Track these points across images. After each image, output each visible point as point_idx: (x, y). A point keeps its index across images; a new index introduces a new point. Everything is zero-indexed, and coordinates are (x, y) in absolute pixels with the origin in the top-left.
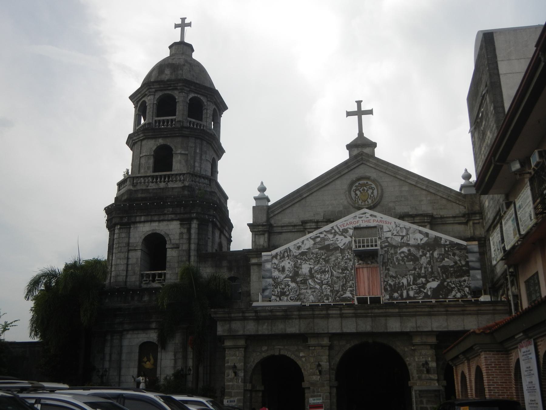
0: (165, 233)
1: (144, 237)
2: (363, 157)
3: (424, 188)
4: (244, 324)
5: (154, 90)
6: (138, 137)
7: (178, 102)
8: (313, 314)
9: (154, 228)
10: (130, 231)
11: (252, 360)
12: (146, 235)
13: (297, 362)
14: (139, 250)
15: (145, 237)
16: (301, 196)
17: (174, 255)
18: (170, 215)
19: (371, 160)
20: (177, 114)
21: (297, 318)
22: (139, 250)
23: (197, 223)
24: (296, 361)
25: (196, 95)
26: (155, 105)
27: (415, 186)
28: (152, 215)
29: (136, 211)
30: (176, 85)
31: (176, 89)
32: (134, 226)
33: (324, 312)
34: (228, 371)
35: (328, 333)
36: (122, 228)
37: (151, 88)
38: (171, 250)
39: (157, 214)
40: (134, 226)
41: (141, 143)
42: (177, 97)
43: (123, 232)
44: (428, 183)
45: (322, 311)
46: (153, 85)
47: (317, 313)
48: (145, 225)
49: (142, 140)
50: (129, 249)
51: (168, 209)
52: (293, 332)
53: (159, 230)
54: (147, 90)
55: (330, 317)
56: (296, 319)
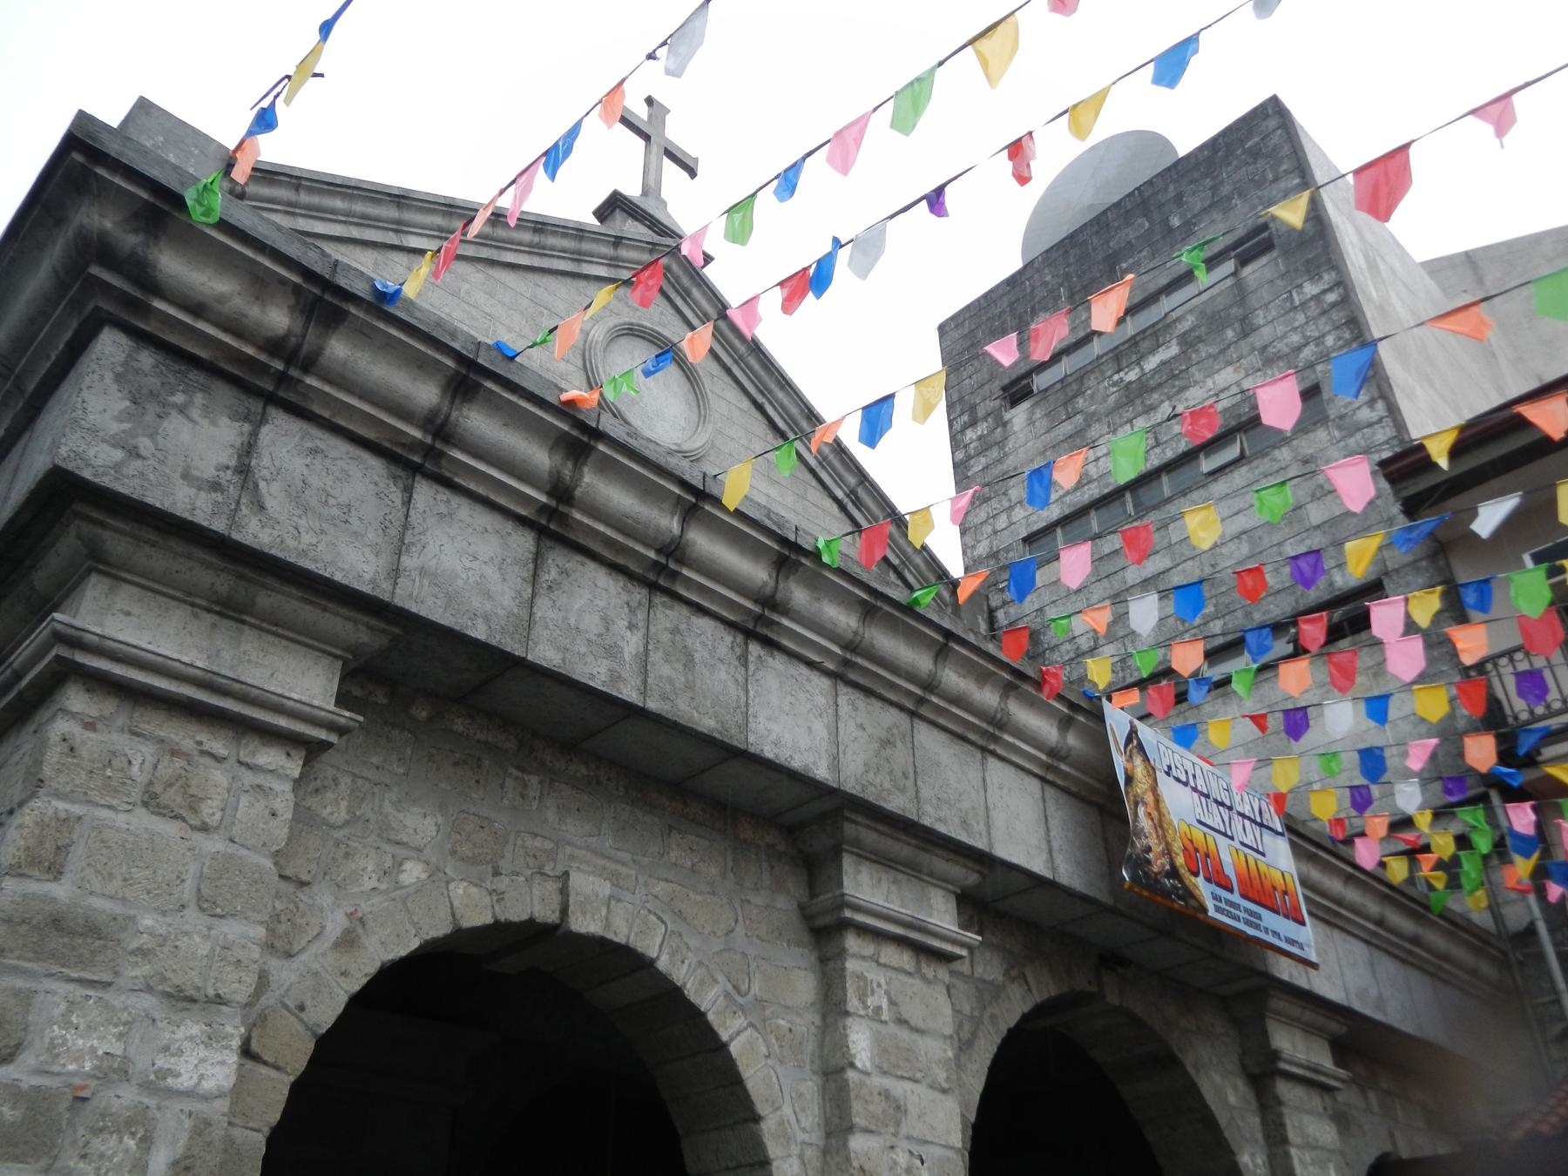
2: (675, 267)
3: (840, 494)
4: (408, 502)
8: (930, 685)
11: (335, 924)
13: (734, 1049)
16: (397, 231)
19: (696, 293)
21: (830, 666)
24: (725, 1037)
27: (812, 471)
33: (988, 697)
34: (20, 983)
35: (983, 860)
44: (861, 483)
45: (983, 678)
47: (952, 678)
52: (797, 764)
55: (1000, 751)
56: (811, 664)
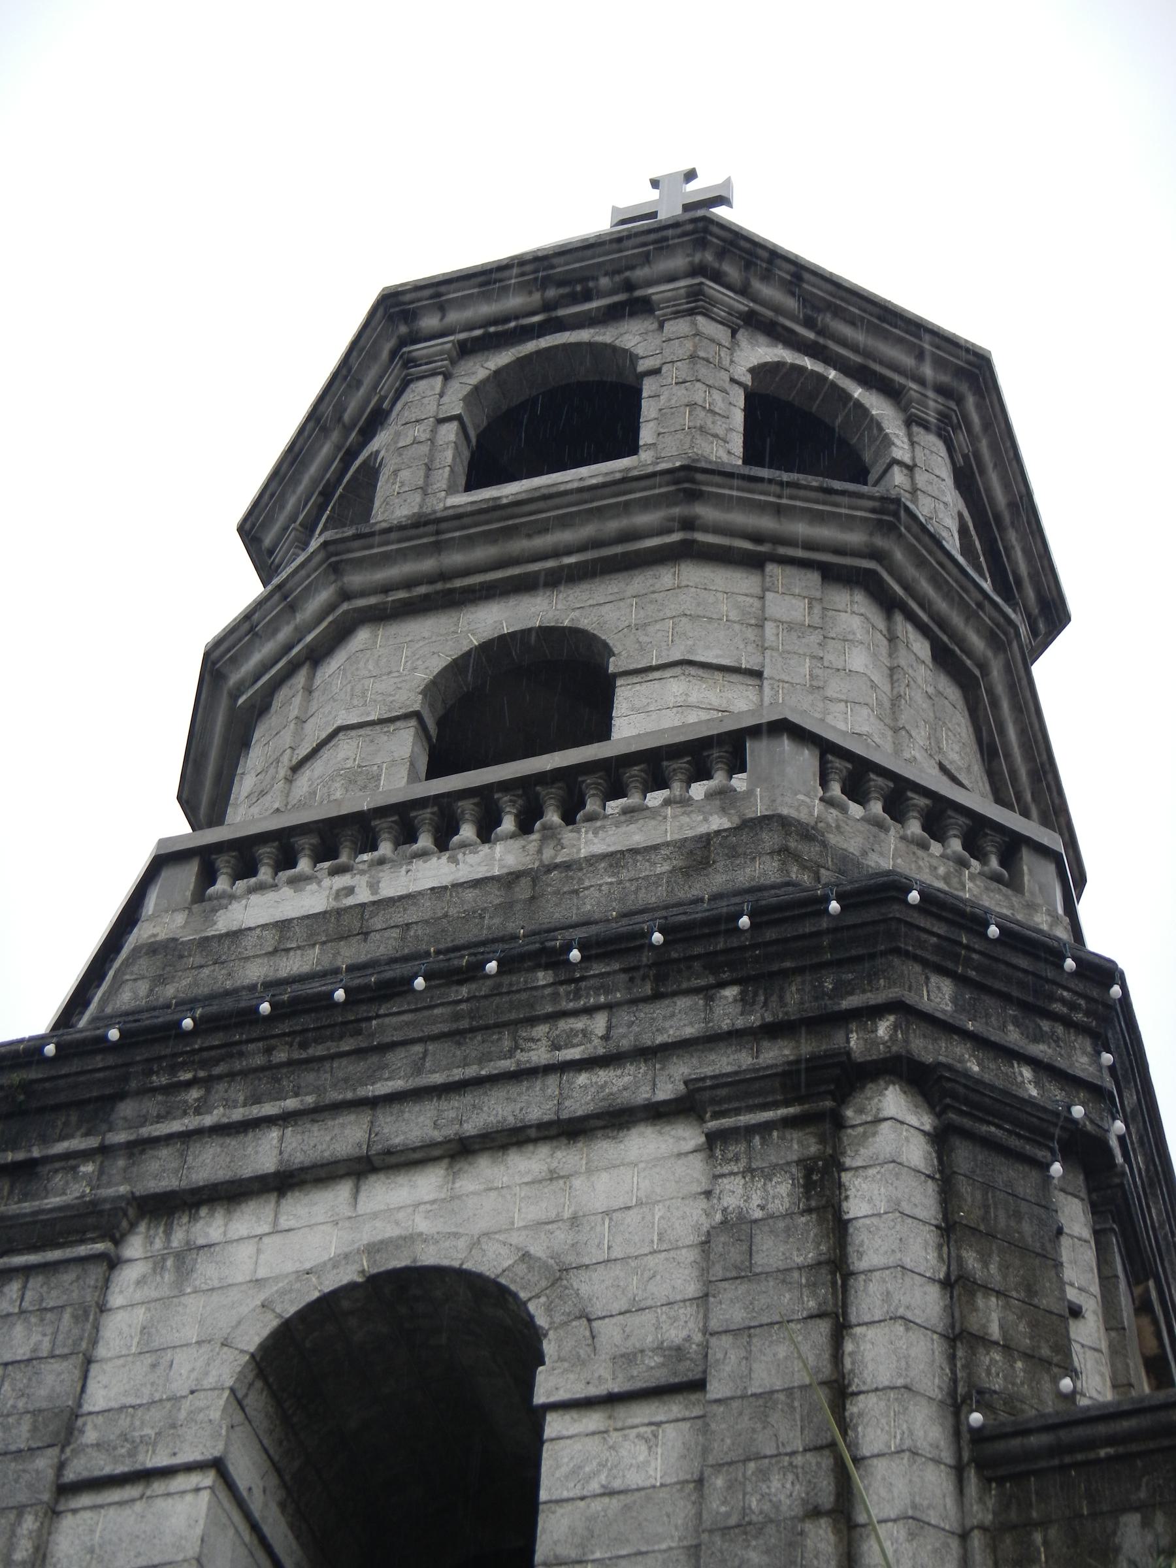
0: (526, 1257)
1: (266, 1332)
5: (446, 343)
6: (285, 633)
7: (656, 372)
9: (390, 1231)
10: (105, 1285)
12: (290, 1310)
14: (194, 1479)
15: (276, 1323)
17: (634, 1479)
18: (583, 1078)
20: (646, 435)
22: (189, 1468)
23: (913, 1120)
25: (808, 363)
26: (454, 426)
28: (373, 1103)
29: (194, 1094)
30: (640, 273)
31: (639, 307)
32: (158, 1244)
36: (27, 1271)
37: (414, 338)
38: (593, 1420)
39: (438, 1078)
40: (158, 1244)
41: (311, 677)
42: (640, 351)
43: (22, 1312)
46: (442, 308)
48: (284, 1223)
49: (316, 656)
50: (70, 1476)
51: (564, 1025)
53: (456, 1235)
54: (394, 354)
